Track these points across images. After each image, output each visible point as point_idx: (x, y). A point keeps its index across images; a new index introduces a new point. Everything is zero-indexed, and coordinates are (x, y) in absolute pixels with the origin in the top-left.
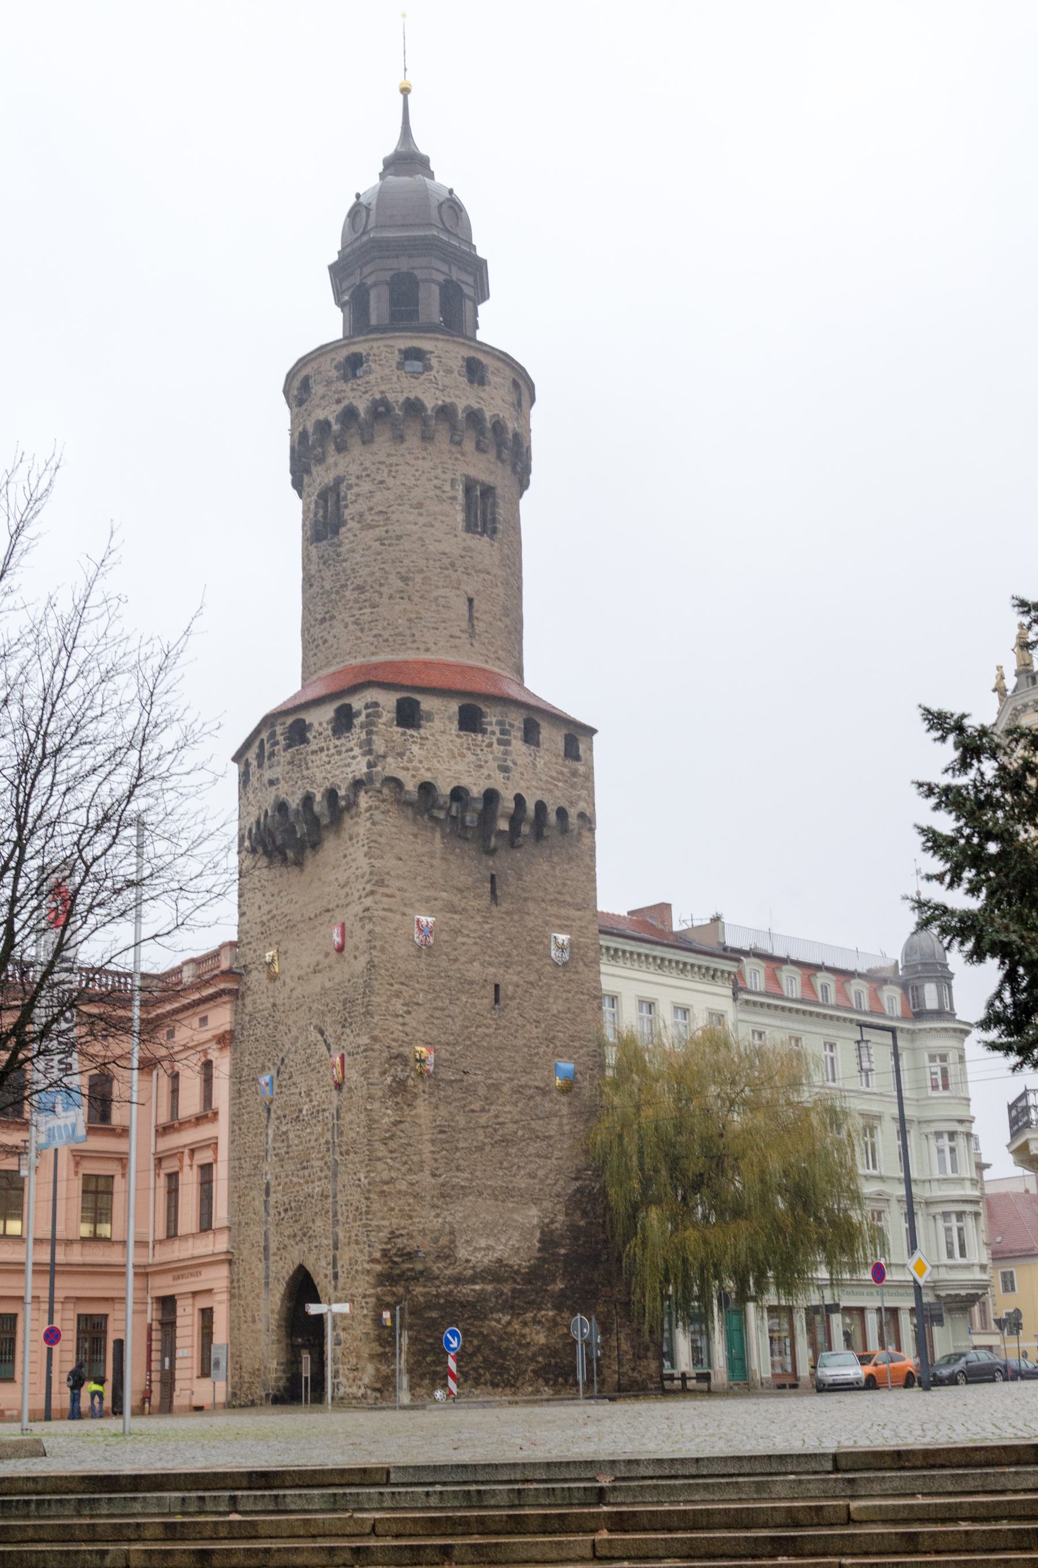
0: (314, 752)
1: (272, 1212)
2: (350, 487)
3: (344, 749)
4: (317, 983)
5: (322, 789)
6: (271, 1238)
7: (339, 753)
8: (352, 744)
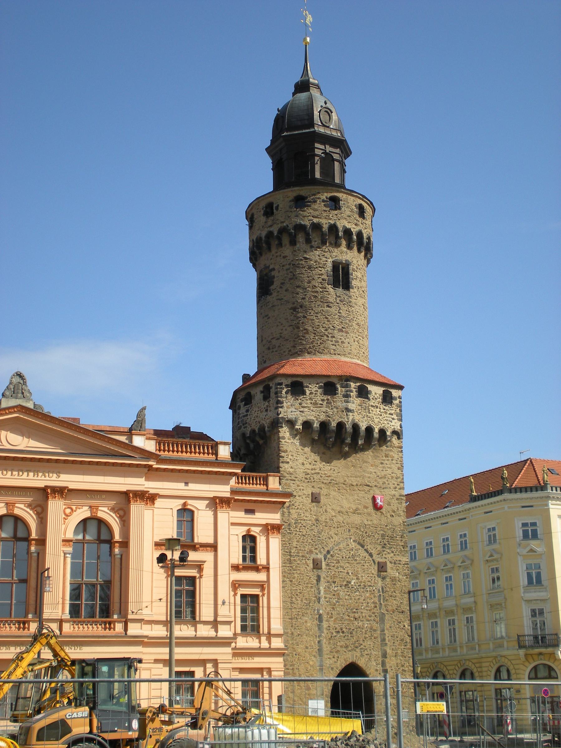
0: (372, 406)
1: (325, 631)
4: (357, 519)
6: (324, 646)
7: (386, 413)
8: (393, 412)
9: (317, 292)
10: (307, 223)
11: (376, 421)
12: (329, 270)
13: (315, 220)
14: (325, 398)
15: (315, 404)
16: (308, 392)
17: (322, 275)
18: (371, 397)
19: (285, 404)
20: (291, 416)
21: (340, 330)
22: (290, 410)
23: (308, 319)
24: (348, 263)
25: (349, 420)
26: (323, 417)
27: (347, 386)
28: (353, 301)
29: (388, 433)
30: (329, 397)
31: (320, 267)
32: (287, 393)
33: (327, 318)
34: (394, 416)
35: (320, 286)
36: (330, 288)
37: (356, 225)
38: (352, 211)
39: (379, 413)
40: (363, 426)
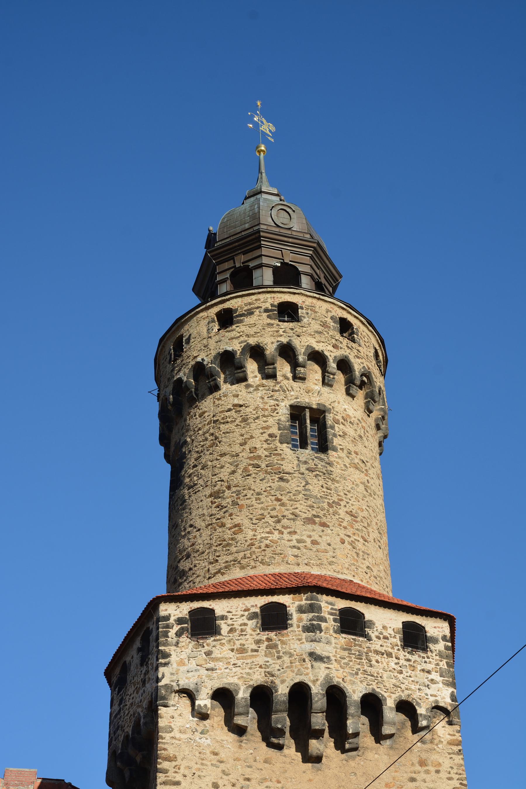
0: (377, 652)
2: (337, 422)
3: (419, 668)
5: (394, 696)
7: (413, 668)
8: (429, 667)
9: (259, 457)
10: (236, 347)
11: (389, 683)
12: (283, 419)
13: (252, 341)
14: (264, 636)
15: (242, 650)
16: (224, 628)
17: (267, 428)
18: (372, 633)
19: (173, 658)
20: (186, 681)
21: (310, 521)
22: (183, 669)
23: (241, 507)
24: (322, 408)
25: (316, 679)
26: (258, 678)
27: (313, 608)
28: (336, 471)
29: (421, 710)
30: (272, 635)
31: (264, 416)
32: (179, 634)
33: (278, 500)
34: (435, 676)
35: (265, 446)
36: (286, 449)
37: (335, 346)
38: (324, 325)
39: (397, 668)
40: (355, 692)
